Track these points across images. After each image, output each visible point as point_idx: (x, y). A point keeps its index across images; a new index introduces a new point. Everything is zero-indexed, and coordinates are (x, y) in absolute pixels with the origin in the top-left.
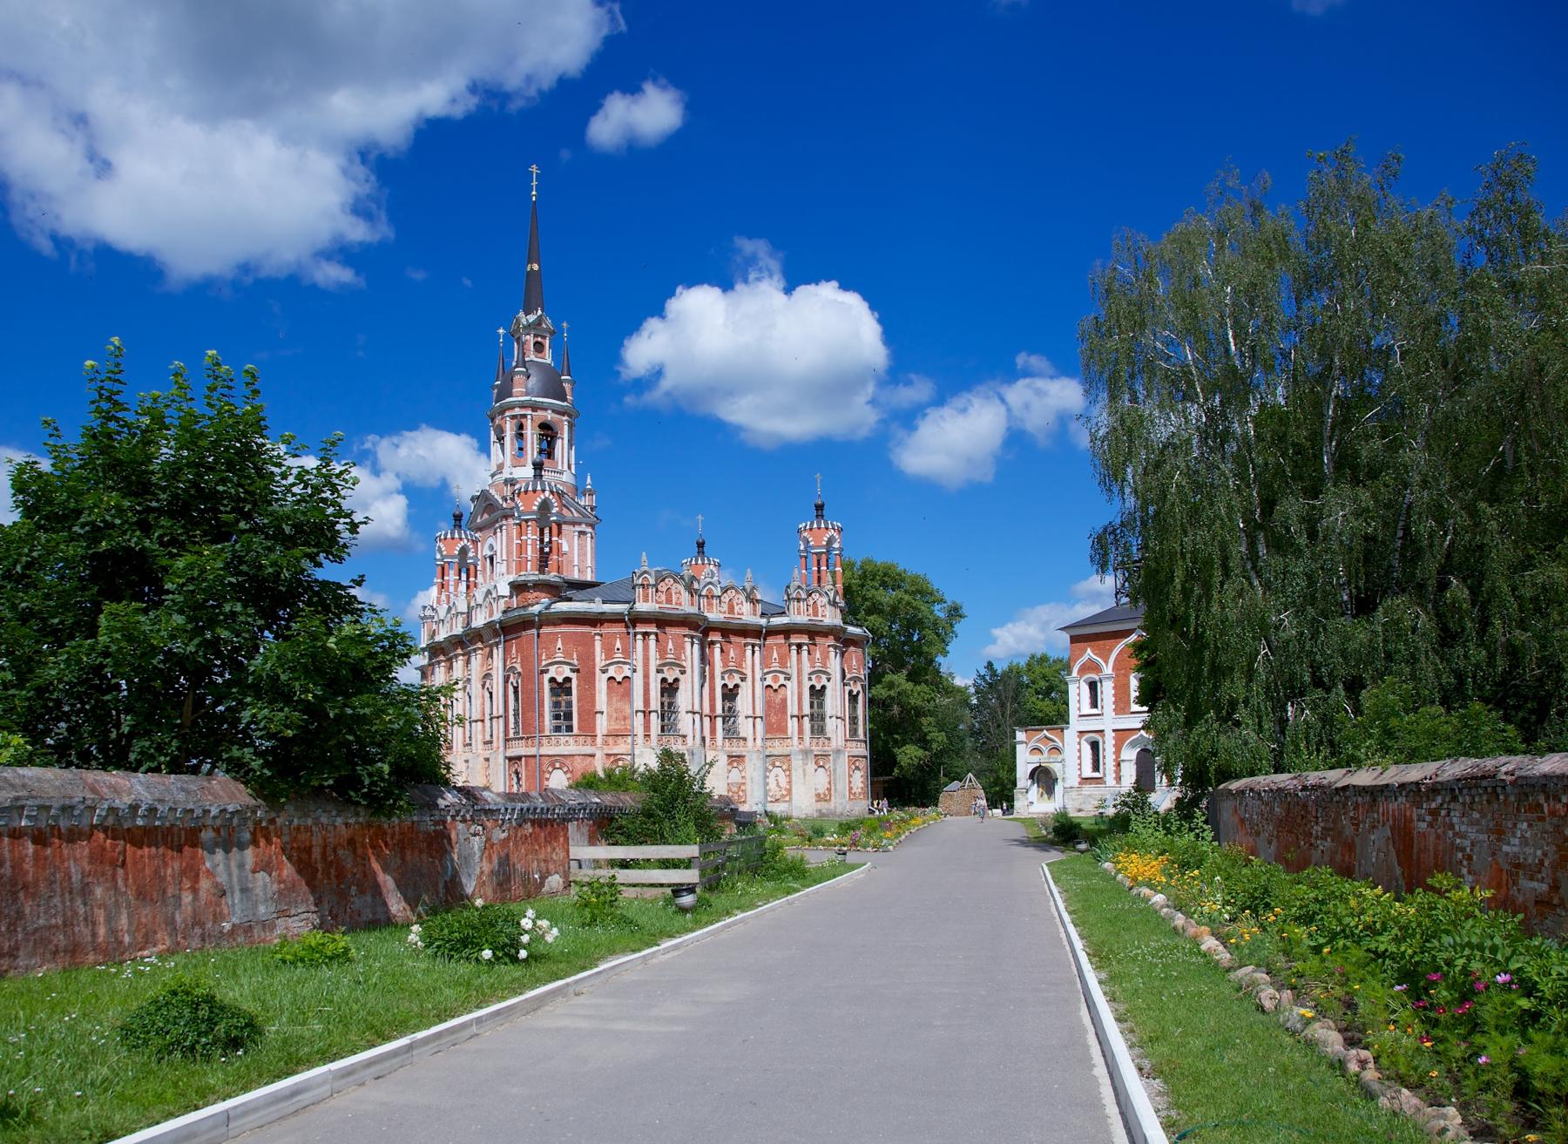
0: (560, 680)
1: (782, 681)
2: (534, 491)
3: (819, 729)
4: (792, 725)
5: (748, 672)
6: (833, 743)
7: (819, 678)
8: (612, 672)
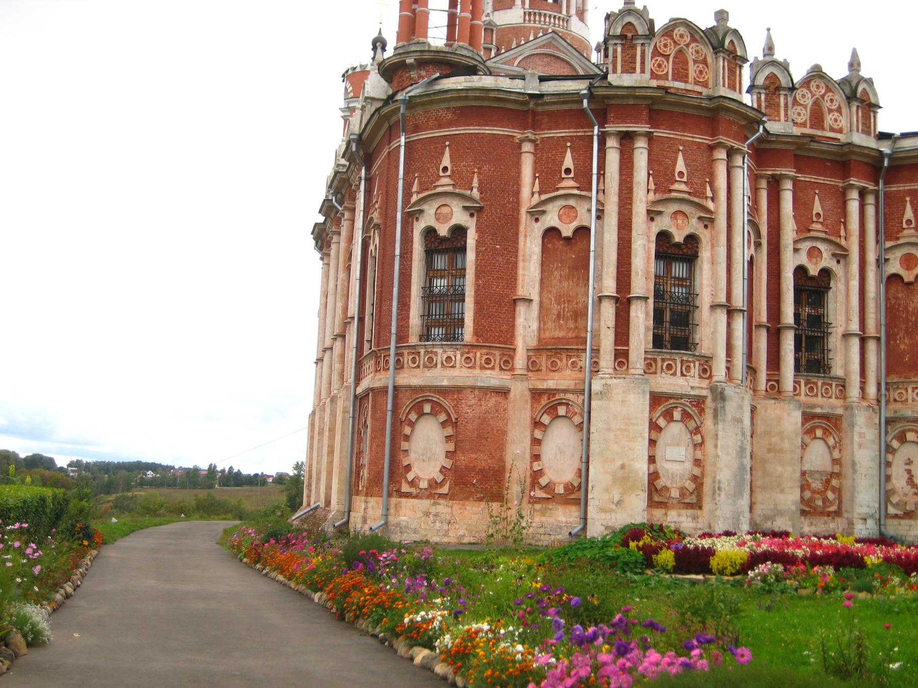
0: (443, 230)
8: (551, 219)
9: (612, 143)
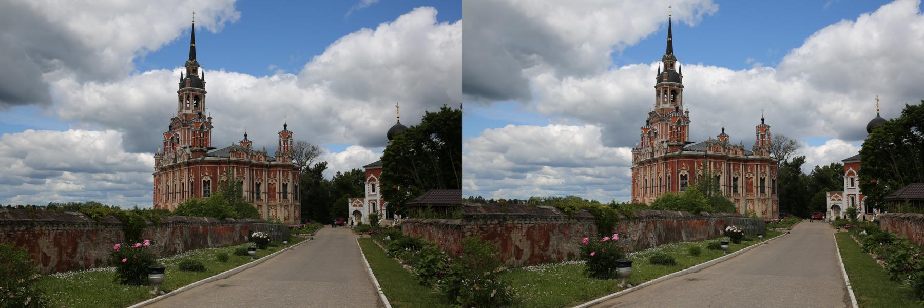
4: (277, 195)
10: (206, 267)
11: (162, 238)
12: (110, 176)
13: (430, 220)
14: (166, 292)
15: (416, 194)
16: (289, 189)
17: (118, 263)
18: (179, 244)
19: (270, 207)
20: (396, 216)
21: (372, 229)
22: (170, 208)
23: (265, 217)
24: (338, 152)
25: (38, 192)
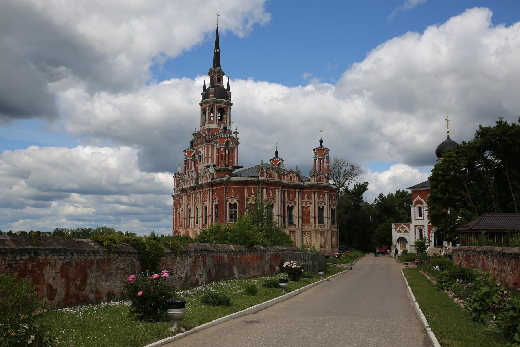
0: (233, 203)
1: (308, 205)
2: (224, 138)
3: (321, 222)
4: (312, 220)
5: (297, 201)
6: (326, 227)
7: (321, 204)
9: (260, 189)
10: (232, 301)
11: (182, 268)
12: (124, 199)
13: (484, 248)
14: (187, 329)
15: (468, 219)
16: (326, 213)
17: (132, 296)
18: (201, 274)
19: (304, 233)
20: (445, 243)
21: (419, 258)
22: (191, 234)
23: (298, 245)
24: (381, 171)
25: (43, 216)
